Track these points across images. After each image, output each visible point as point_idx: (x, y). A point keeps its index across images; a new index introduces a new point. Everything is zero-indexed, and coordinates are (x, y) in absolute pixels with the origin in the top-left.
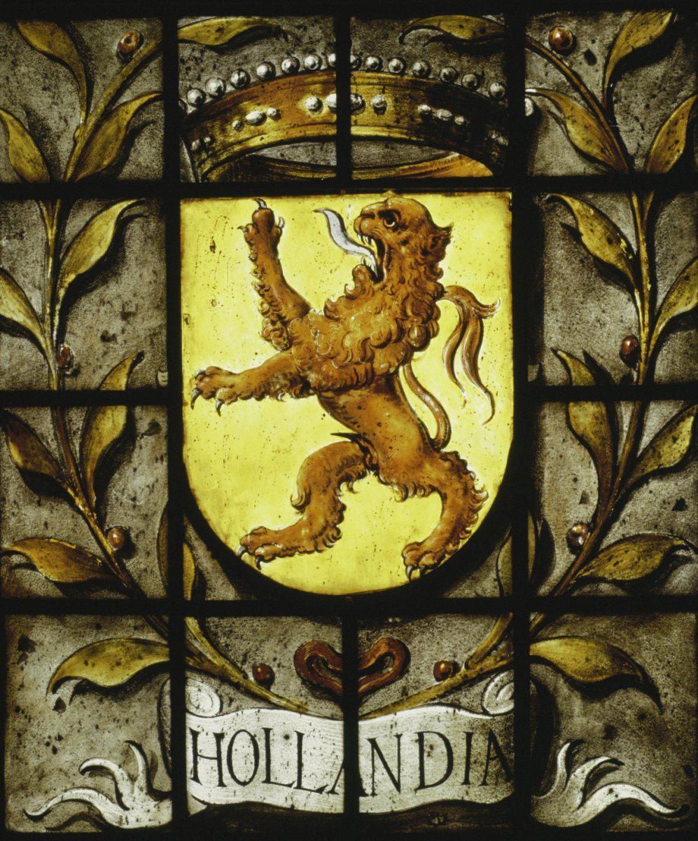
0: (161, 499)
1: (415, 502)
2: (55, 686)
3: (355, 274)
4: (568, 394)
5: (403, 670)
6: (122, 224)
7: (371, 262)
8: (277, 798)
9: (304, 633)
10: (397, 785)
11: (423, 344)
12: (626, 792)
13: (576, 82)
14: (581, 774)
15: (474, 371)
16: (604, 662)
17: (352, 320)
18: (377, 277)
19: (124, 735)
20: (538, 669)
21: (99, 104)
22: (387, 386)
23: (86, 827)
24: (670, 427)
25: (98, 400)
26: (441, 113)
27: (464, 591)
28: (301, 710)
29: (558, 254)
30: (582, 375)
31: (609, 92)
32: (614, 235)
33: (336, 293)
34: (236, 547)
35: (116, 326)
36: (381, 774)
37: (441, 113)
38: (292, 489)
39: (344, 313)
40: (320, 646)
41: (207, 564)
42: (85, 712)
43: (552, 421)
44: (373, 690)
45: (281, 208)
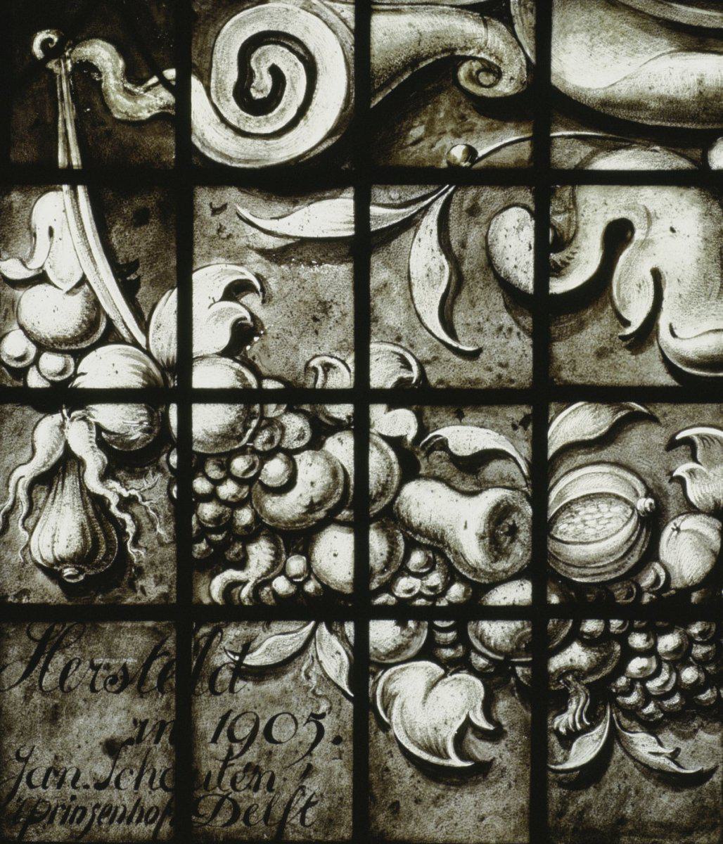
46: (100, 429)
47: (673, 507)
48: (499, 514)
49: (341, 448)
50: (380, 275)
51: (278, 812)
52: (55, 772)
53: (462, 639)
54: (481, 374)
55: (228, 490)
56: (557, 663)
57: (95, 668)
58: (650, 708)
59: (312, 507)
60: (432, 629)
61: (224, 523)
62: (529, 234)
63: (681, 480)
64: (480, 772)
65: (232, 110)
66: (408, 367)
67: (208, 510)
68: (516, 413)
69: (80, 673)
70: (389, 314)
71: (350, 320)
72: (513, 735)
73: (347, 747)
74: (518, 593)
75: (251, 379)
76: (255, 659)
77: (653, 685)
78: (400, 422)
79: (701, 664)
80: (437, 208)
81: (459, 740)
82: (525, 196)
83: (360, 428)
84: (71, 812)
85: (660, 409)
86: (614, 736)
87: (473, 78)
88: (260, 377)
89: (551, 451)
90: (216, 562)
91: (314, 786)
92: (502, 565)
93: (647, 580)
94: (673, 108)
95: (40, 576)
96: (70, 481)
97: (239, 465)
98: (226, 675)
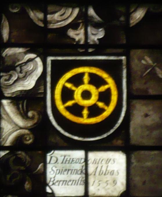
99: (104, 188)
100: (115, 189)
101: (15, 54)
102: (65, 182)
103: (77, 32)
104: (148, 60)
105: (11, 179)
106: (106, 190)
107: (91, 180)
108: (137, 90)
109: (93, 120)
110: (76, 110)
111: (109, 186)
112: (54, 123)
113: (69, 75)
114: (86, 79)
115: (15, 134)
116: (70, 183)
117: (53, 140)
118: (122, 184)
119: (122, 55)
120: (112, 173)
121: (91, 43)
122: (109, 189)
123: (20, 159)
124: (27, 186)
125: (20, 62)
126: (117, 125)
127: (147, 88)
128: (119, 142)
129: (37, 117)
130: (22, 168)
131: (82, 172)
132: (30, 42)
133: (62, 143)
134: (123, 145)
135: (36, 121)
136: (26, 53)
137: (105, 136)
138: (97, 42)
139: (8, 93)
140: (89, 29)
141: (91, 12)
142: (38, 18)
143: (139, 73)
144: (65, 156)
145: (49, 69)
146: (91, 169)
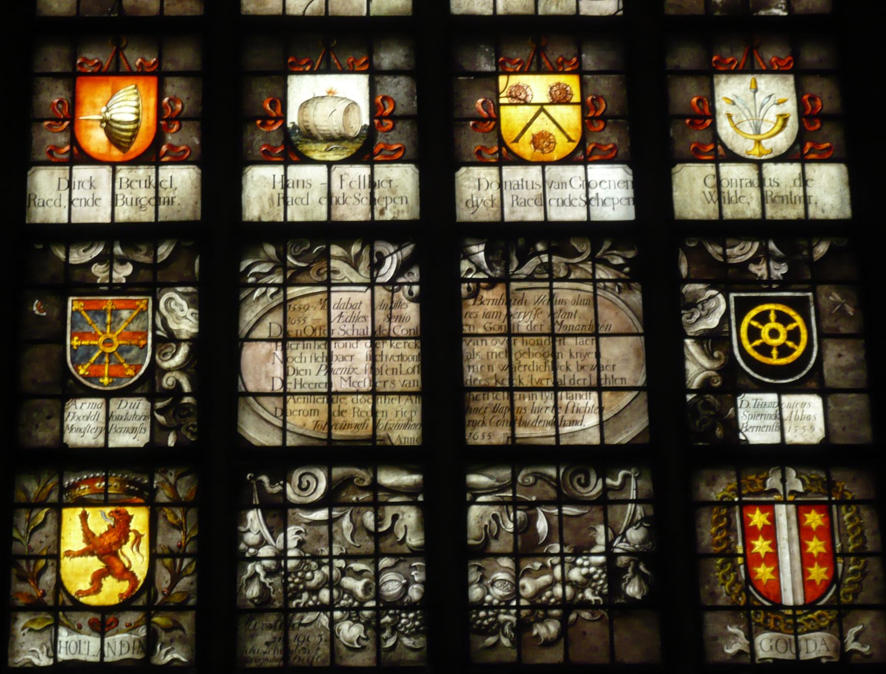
0: (54, 582)
1: (122, 583)
2: (23, 629)
3: (108, 526)
4: (163, 556)
5: (117, 624)
6: (47, 514)
7: (112, 523)
8: (82, 658)
9: (91, 616)
10: (114, 654)
11: (125, 543)
12: (176, 656)
13: (167, 480)
14: (164, 651)
15: (138, 550)
16: (171, 623)
17: (107, 538)
18: (113, 527)
19: (41, 642)
20: (153, 625)
21: (42, 485)
22: (115, 555)
23: (29, 665)
24: (189, 565)
25: (38, 557)
26: (132, 487)
27: (134, 604)
28: (89, 635)
29: (161, 522)
30: (167, 551)
31: (176, 483)
32: (176, 517)
33: (103, 531)
34: (73, 594)
35: (44, 539)
36: (110, 652)
37: (132, 487)
38: (89, 579)
39: (104, 536)
40: (95, 619)
41: (65, 598)
42: (30, 636)
43: (159, 563)
44: (108, 630)
45: (89, 510)
46: (264, 566)
47: (411, 582)
48: (366, 586)
49: (326, 570)
50: (335, 528)
51: (311, 659)
52: (253, 650)
53: (358, 615)
54: (361, 551)
55: (297, 580)
56: (383, 621)
57: (263, 624)
58: (407, 632)
59: (318, 584)
60: (350, 613)
61: (296, 588)
62: (372, 517)
63: (413, 576)
64: (363, 648)
65: (297, 490)
66: (342, 550)
67: (292, 585)
68: (371, 560)
69: (259, 625)
70: (338, 538)
71: (327, 539)
72: (372, 639)
73: (328, 643)
74: (372, 604)
75: (303, 554)
76: (305, 621)
77: (408, 626)
78: (340, 563)
79: (420, 620)
80: (349, 512)
81: (358, 640)
82: (372, 508)
83: (331, 565)
84: (257, 660)
85: (407, 559)
86: (398, 639)
87: (358, 481)
88: (305, 553)
89: (380, 569)
90: (294, 597)
91: (320, 653)
92: (368, 597)
93: (405, 600)
94: (408, 487)
95: (249, 602)
96: (256, 579)
97: (300, 574)
98: (297, 626)
99: (801, 434)
100: (814, 435)
101: (695, 291)
102: (759, 428)
103: (759, 267)
104: (836, 297)
105: (700, 424)
106: (804, 436)
107: (787, 425)
108: (828, 328)
109: (783, 361)
110: (765, 350)
111: (806, 433)
112: (742, 364)
113: (754, 313)
114: (772, 316)
115: (701, 376)
116: (764, 429)
117: (742, 382)
118: (821, 430)
119: (808, 291)
120: (809, 418)
121: (775, 278)
122: (807, 435)
123: (709, 403)
124: (719, 432)
125: (702, 299)
126: (810, 366)
127: (838, 326)
128: (813, 385)
129: (723, 357)
130: (712, 413)
131: (776, 417)
132: (711, 278)
133: (752, 385)
134: (818, 387)
135: (722, 362)
136: (707, 289)
137: (798, 377)
138: (781, 278)
139: (691, 331)
140: (771, 264)
141: (772, 246)
142: (716, 252)
143: (828, 310)
144: (757, 400)
145: (732, 306)
146: (786, 414)
